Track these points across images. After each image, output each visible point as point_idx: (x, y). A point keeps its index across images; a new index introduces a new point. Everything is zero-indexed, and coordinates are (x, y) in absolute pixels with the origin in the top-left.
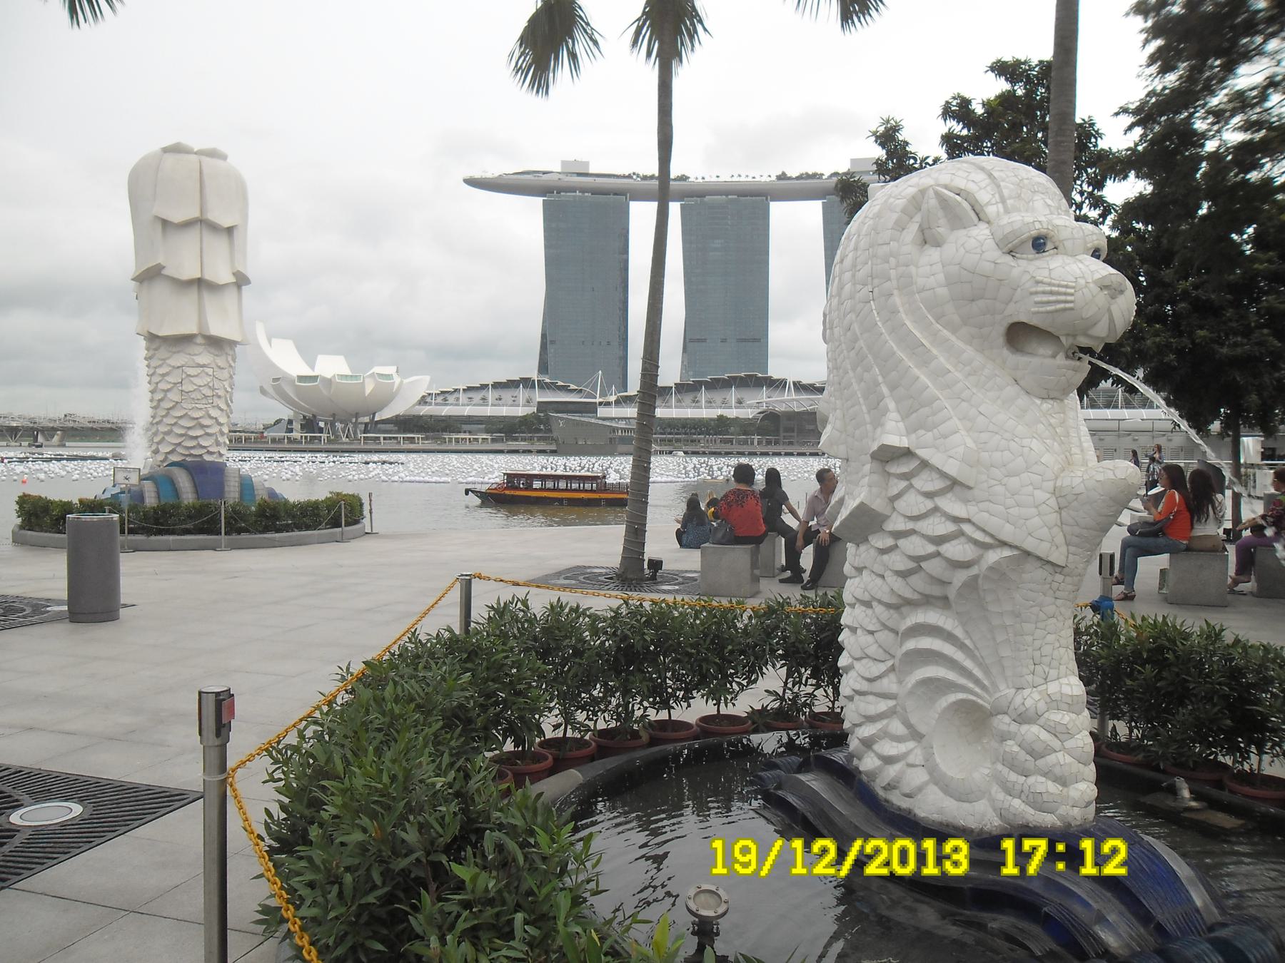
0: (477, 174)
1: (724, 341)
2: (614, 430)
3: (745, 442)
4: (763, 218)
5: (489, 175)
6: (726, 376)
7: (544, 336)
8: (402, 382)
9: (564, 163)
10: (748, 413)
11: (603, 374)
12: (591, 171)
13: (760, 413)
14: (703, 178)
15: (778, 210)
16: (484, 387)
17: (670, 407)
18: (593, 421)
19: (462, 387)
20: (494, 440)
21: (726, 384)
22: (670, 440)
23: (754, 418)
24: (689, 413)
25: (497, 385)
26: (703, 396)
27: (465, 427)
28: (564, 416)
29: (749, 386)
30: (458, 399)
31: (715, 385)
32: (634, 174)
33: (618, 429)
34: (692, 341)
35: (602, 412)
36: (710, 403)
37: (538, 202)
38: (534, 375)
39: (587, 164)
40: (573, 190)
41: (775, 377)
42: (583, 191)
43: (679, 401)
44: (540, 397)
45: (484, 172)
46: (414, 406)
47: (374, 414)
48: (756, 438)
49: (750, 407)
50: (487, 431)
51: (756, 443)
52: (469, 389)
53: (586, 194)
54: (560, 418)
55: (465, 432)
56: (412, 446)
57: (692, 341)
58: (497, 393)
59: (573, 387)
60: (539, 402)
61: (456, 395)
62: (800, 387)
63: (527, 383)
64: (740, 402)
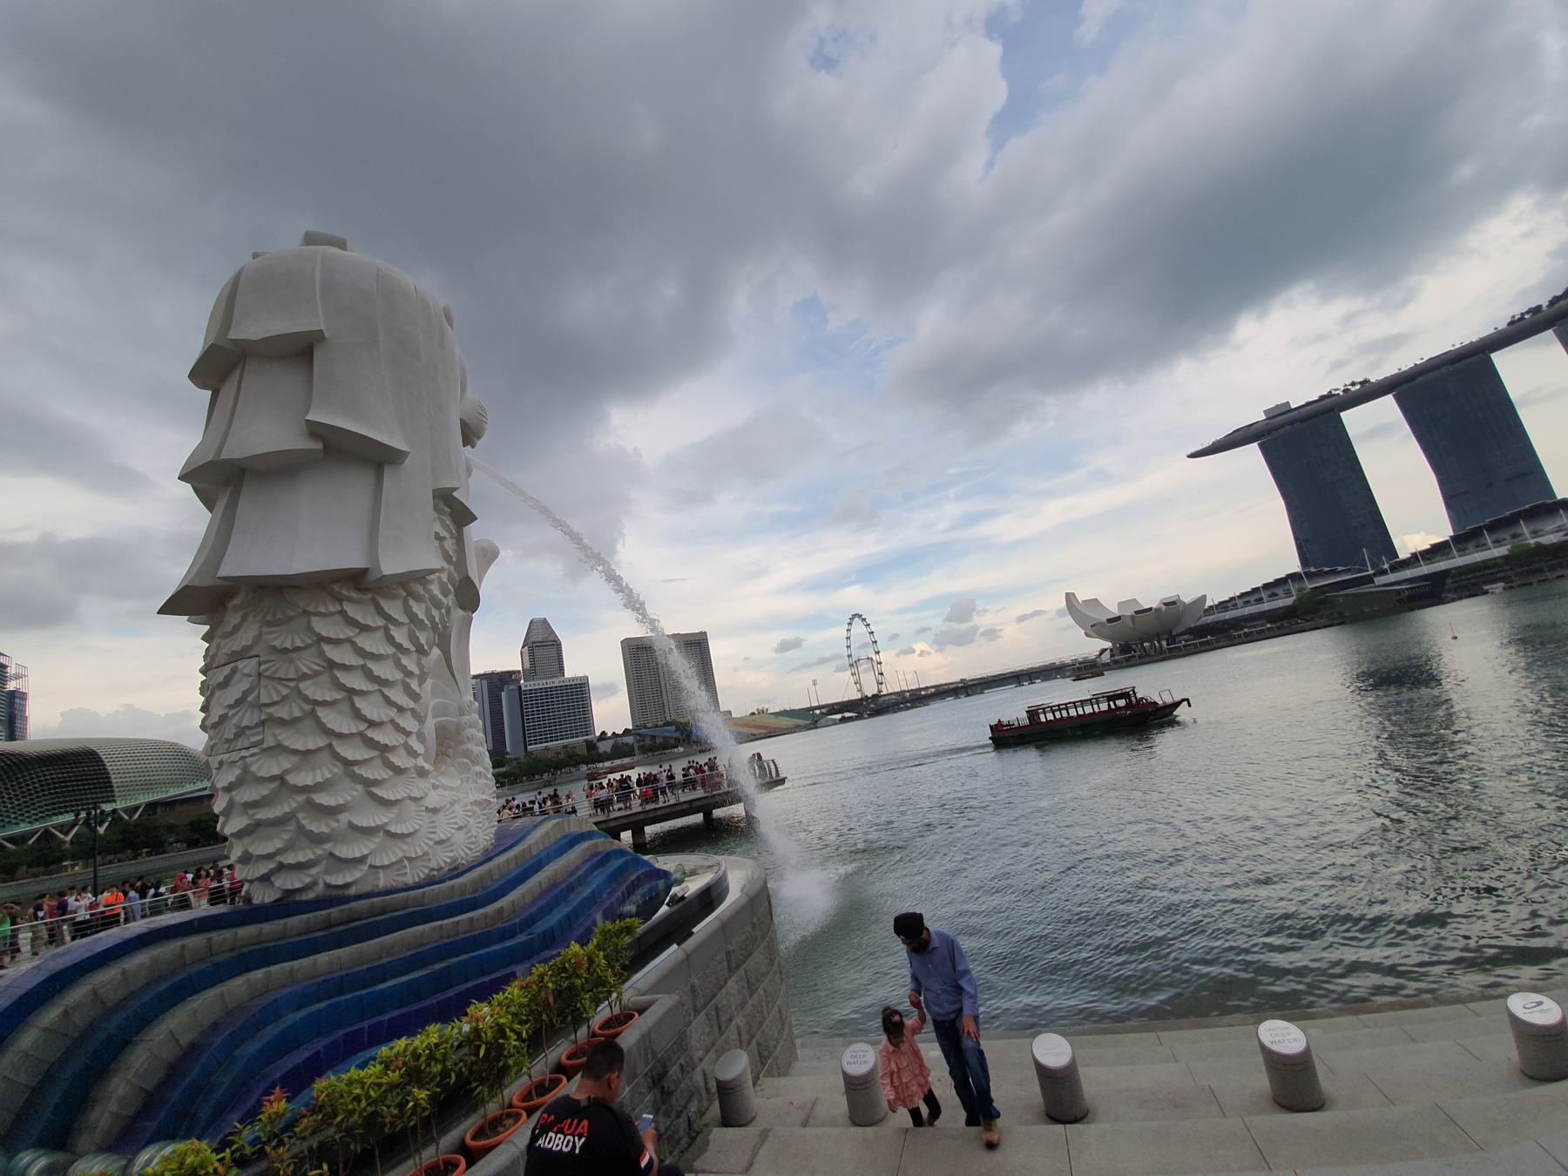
2: (1398, 591)
11: (1368, 550)
12: (1293, 407)
16: (1255, 590)
18: (1373, 590)
21: (1512, 521)
24: (1477, 557)
25: (1266, 586)
28: (1341, 593)
31: (1493, 527)
35: (1379, 580)
36: (1497, 542)
37: (1254, 447)
40: (1282, 426)
44: (1309, 585)
47: (1171, 632)
58: (1269, 593)
59: (1340, 568)
63: (1293, 577)
64: (1535, 533)
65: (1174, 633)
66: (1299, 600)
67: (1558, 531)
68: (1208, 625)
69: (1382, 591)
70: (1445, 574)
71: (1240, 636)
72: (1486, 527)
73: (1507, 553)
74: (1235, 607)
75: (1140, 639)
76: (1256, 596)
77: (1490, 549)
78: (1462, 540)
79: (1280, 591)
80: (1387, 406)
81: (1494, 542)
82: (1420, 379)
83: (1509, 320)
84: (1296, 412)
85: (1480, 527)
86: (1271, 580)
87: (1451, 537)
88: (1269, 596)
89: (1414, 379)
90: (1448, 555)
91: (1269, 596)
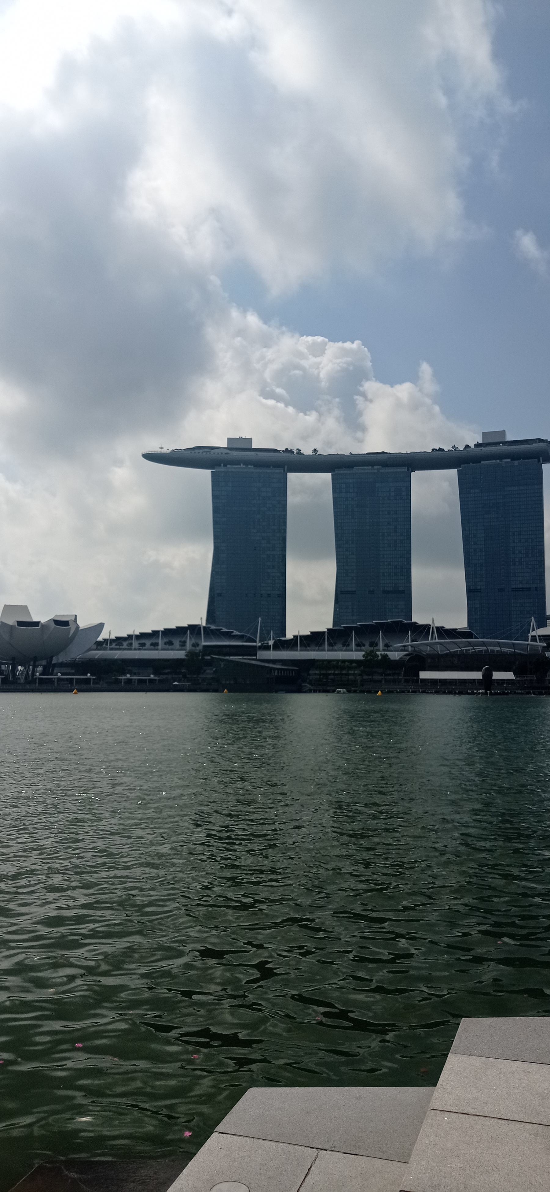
5: (164, 451)
9: (230, 440)
10: (395, 655)
12: (254, 446)
13: (406, 655)
15: (417, 477)
16: (155, 633)
18: (253, 662)
30: (131, 644)
33: (275, 669)
35: (263, 655)
42: (247, 463)
43: (330, 644)
45: (161, 448)
57: (342, 592)
62: (442, 632)
63: (194, 629)
65: (54, 661)
66: (191, 655)
67: (402, 651)
72: (355, 628)
74: (130, 647)
75: (13, 659)
82: (356, 470)
84: (253, 453)
85: (351, 629)
86: (173, 627)
87: (328, 630)
89: (352, 467)
91: (165, 643)
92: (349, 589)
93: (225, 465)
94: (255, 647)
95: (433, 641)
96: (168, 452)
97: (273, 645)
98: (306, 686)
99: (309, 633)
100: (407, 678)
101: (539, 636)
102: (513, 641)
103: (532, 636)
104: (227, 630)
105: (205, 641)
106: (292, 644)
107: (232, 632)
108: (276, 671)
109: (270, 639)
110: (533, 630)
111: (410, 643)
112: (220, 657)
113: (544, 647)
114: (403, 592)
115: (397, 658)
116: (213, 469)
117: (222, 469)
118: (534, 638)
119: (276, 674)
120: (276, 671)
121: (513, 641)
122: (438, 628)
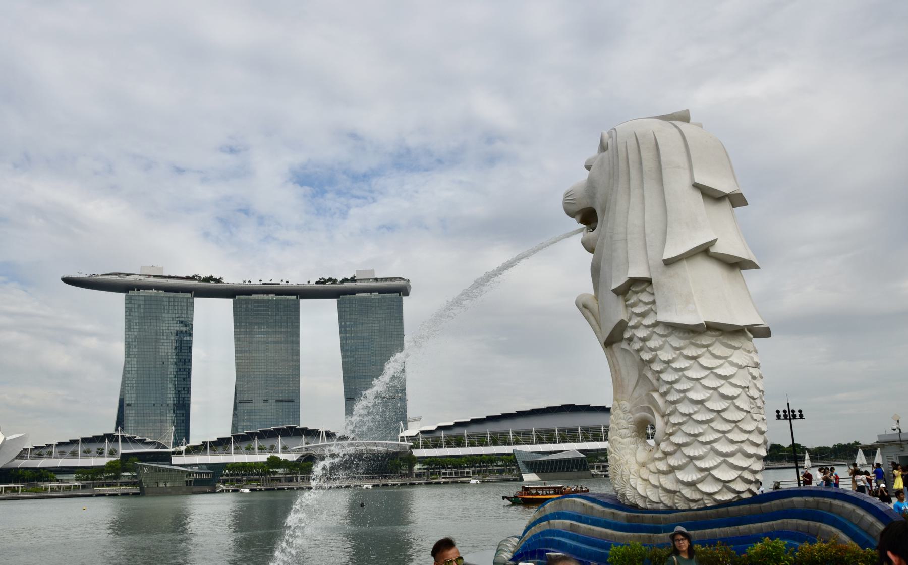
0: (74, 274)
1: (266, 401)
2: (189, 474)
3: (290, 480)
4: (295, 310)
6: (272, 428)
7: (121, 401)
8: (5, 439)
10: (292, 457)
14: (250, 281)
16: (73, 442)
17: (229, 453)
18: (167, 466)
19: (55, 443)
20: (83, 487)
22: (232, 481)
23: (297, 460)
25: (85, 440)
26: (256, 444)
27: (59, 477)
29: (290, 436)
31: (263, 435)
32: (197, 276)
33: (193, 473)
34: (241, 402)
35: (175, 460)
36: (261, 449)
38: (111, 430)
39: (162, 269)
41: (310, 427)
42: (158, 288)
43: (236, 449)
44: (122, 449)
46: (13, 460)
48: (299, 476)
49: (294, 451)
50: (77, 479)
51: (299, 479)
52: (60, 444)
53: (160, 291)
54: (145, 466)
55: (58, 481)
56: (14, 495)
57: (241, 402)
58: (85, 447)
59: (148, 440)
60: (122, 454)
61: (49, 450)
63: (111, 438)
64: (285, 449)
68: (17, 469)
69: (175, 470)
70: (224, 466)
71: (46, 489)
72: (256, 434)
73: (265, 460)
76: (72, 448)
77: (254, 453)
78: (241, 440)
79: (94, 448)
80: (226, 305)
81: (259, 449)
83: (318, 280)
87: (232, 436)
88: (85, 452)
89: (251, 295)
90: (227, 451)
91: (85, 452)
92: (245, 399)
93: (138, 290)
94: (168, 453)
95: (323, 444)
96: (86, 277)
97: (186, 450)
98: (220, 486)
99: (216, 440)
100: (303, 475)
101: (406, 437)
102: (387, 442)
103: (401, 437)
104: (140, 438)
105: (123, 449)
106: (201, 449)
107: (145, 440)
108: (195, 475)
109: (182, 445)
110: (402, 432)
111: (304, 446)
112: (144, 463)
113: (411, 446)
114: (292, 401)
115: (295, 460)
116: (128, 293)
117: (136, 292)
118: (402, 439)
119: (195, 477)
120: (195, 475)
121: (387, 442)
122: (326, 432)
